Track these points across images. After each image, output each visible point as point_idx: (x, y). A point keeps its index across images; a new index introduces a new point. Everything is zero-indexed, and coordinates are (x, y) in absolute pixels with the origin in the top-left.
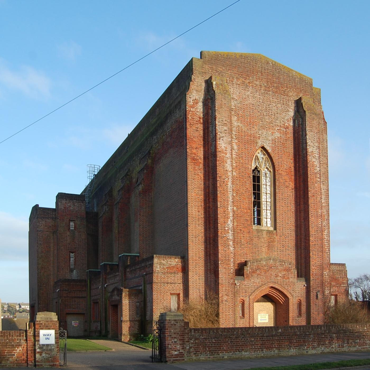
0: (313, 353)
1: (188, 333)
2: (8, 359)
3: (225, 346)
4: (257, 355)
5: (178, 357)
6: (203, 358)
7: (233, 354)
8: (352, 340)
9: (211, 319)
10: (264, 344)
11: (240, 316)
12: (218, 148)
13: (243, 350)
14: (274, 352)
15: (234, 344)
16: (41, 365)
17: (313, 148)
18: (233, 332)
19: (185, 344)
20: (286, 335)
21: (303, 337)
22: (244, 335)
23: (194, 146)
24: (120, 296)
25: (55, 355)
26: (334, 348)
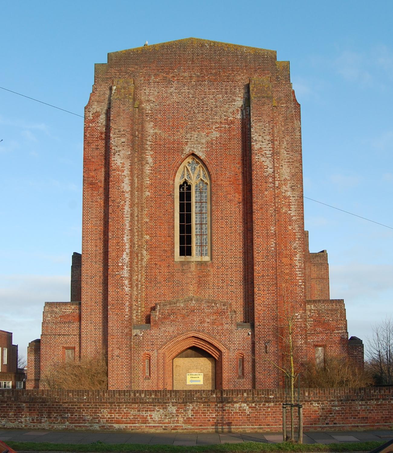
8: (58, 413)
12: (112, 166)
17: (262, 144)
26: (24, 423)
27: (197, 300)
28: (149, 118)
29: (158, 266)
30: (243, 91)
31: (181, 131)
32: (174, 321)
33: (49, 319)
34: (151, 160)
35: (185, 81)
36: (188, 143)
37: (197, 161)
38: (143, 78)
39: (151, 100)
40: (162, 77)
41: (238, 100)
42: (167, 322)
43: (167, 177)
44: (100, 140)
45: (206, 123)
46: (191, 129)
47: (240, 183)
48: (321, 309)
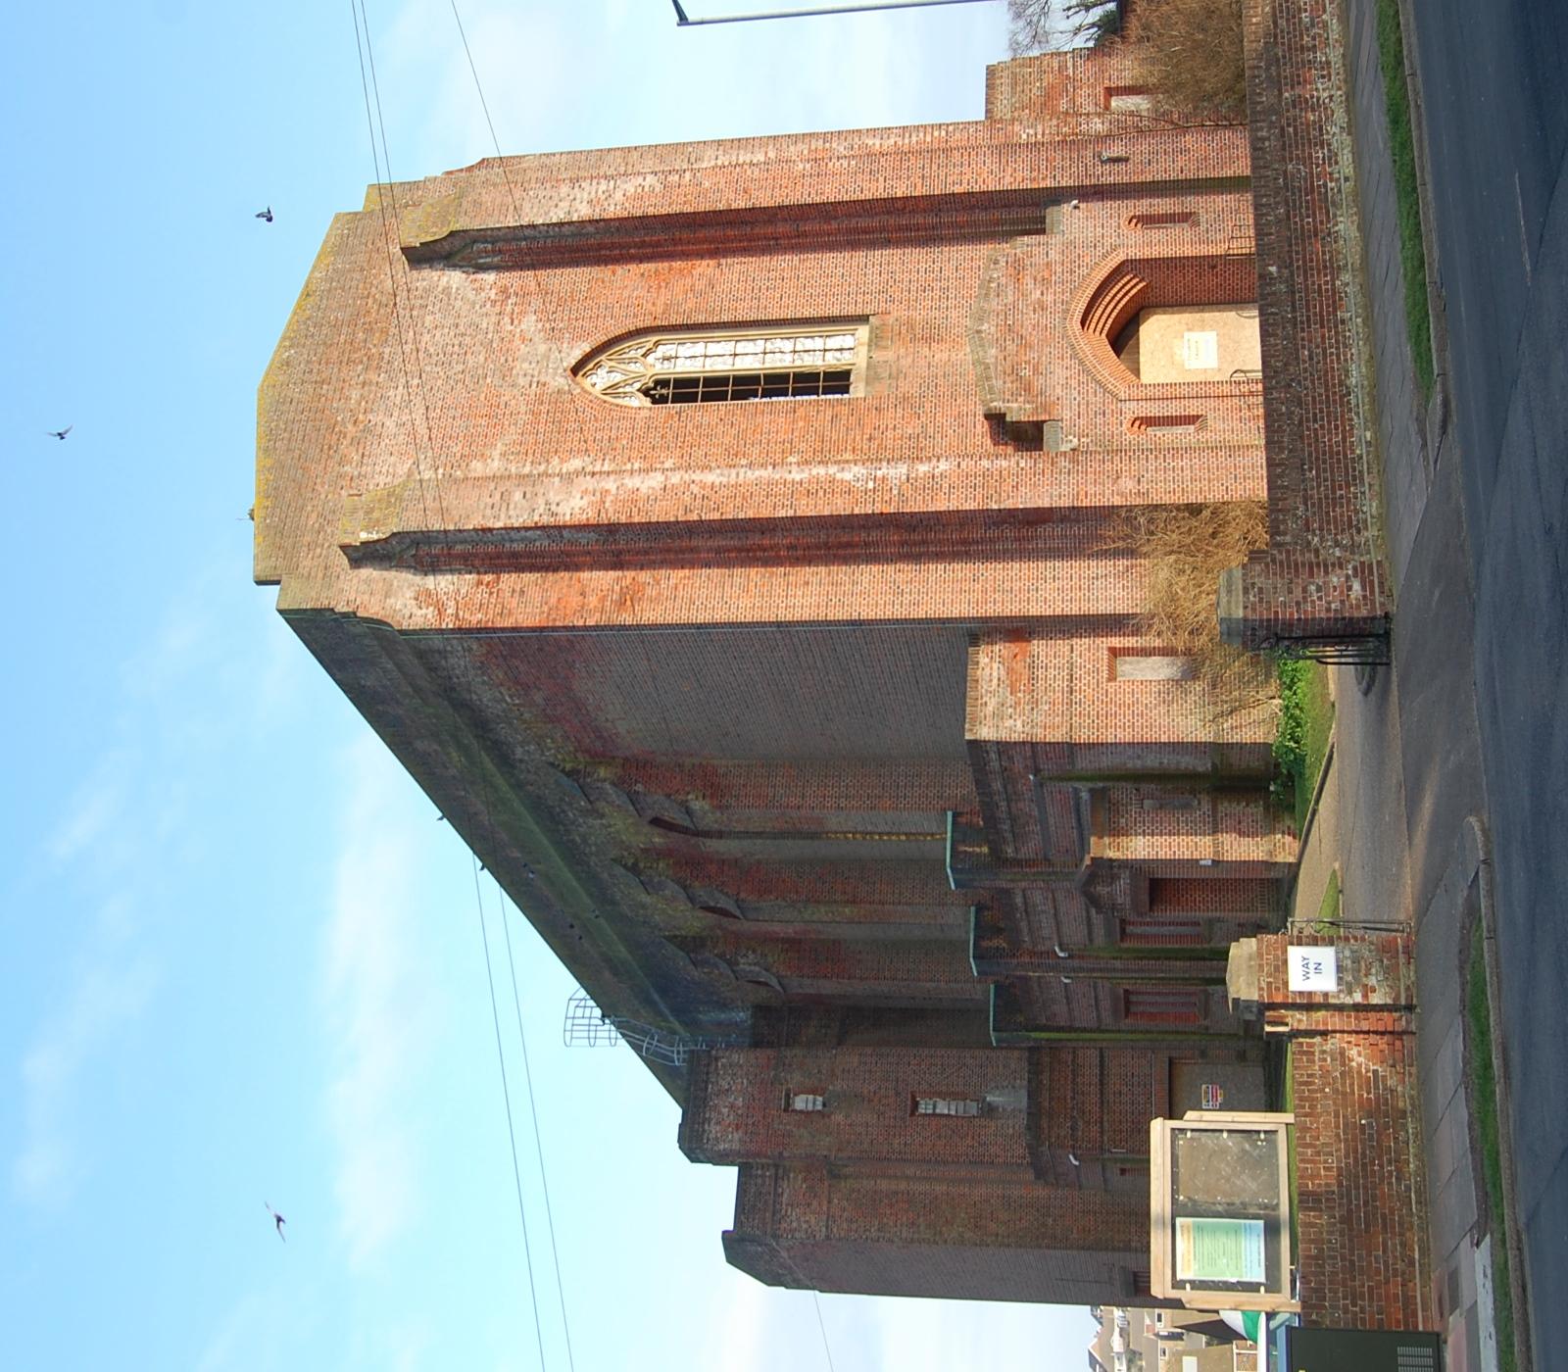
0: (1351, 160)
1: (1288, 551)
2: (1392, 1091)
3: (1330, 440)
4: (1359, 340)
5: (1372, 582)
6: (1374, 504)
7: (1357, 414)
8: (1301, 35)
9: (1211, 530)
10: (1322, 316)
11: (1197, 431)
12: (588, 519)
13: (1341, 383)
14: (1348, 284)
15: (1321, 411)
16: (1408, 988)
18: (1283, 414)
19: (1325, 560)
20: (1287, 249)
21: (1294, 194)
22: (1292, 380)
23: (575, 601)
24: (1120, 867)
25: (1373, 947)
26: (1332, 92)
27: (981, 320)
28: (458, 473)
29: (876, 434)
30: (426, 273)
31: (506, 398)
32: (1036, 370)
33: (1019, 723)
34: (577, 461)
35: (372, 396)
36: (543, 380)
37: (591, 366)
38: (343, 492)
39: (409, 469)
40: (351, 448)
41: (448, 282)
42: (1038, 383)
43: (626, 424)
44: (498, 584)
45: (494, 345)
46: (504, 376)
47: (666, 264)
48: (1009, 107)
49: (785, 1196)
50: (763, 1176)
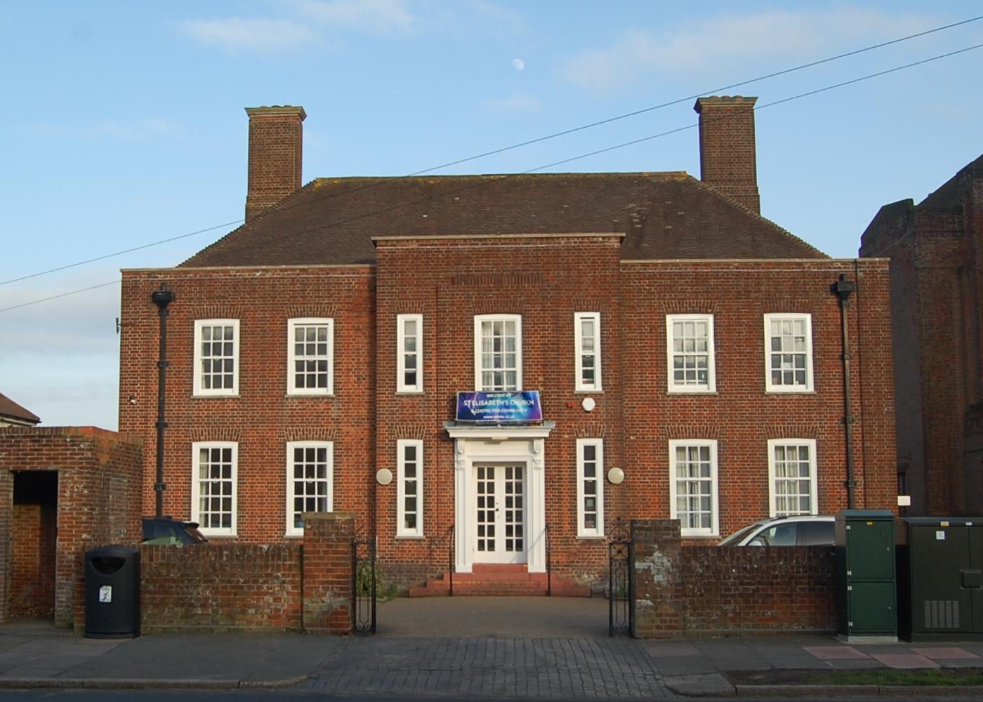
49: (942, 238)
50: (954, 222)
